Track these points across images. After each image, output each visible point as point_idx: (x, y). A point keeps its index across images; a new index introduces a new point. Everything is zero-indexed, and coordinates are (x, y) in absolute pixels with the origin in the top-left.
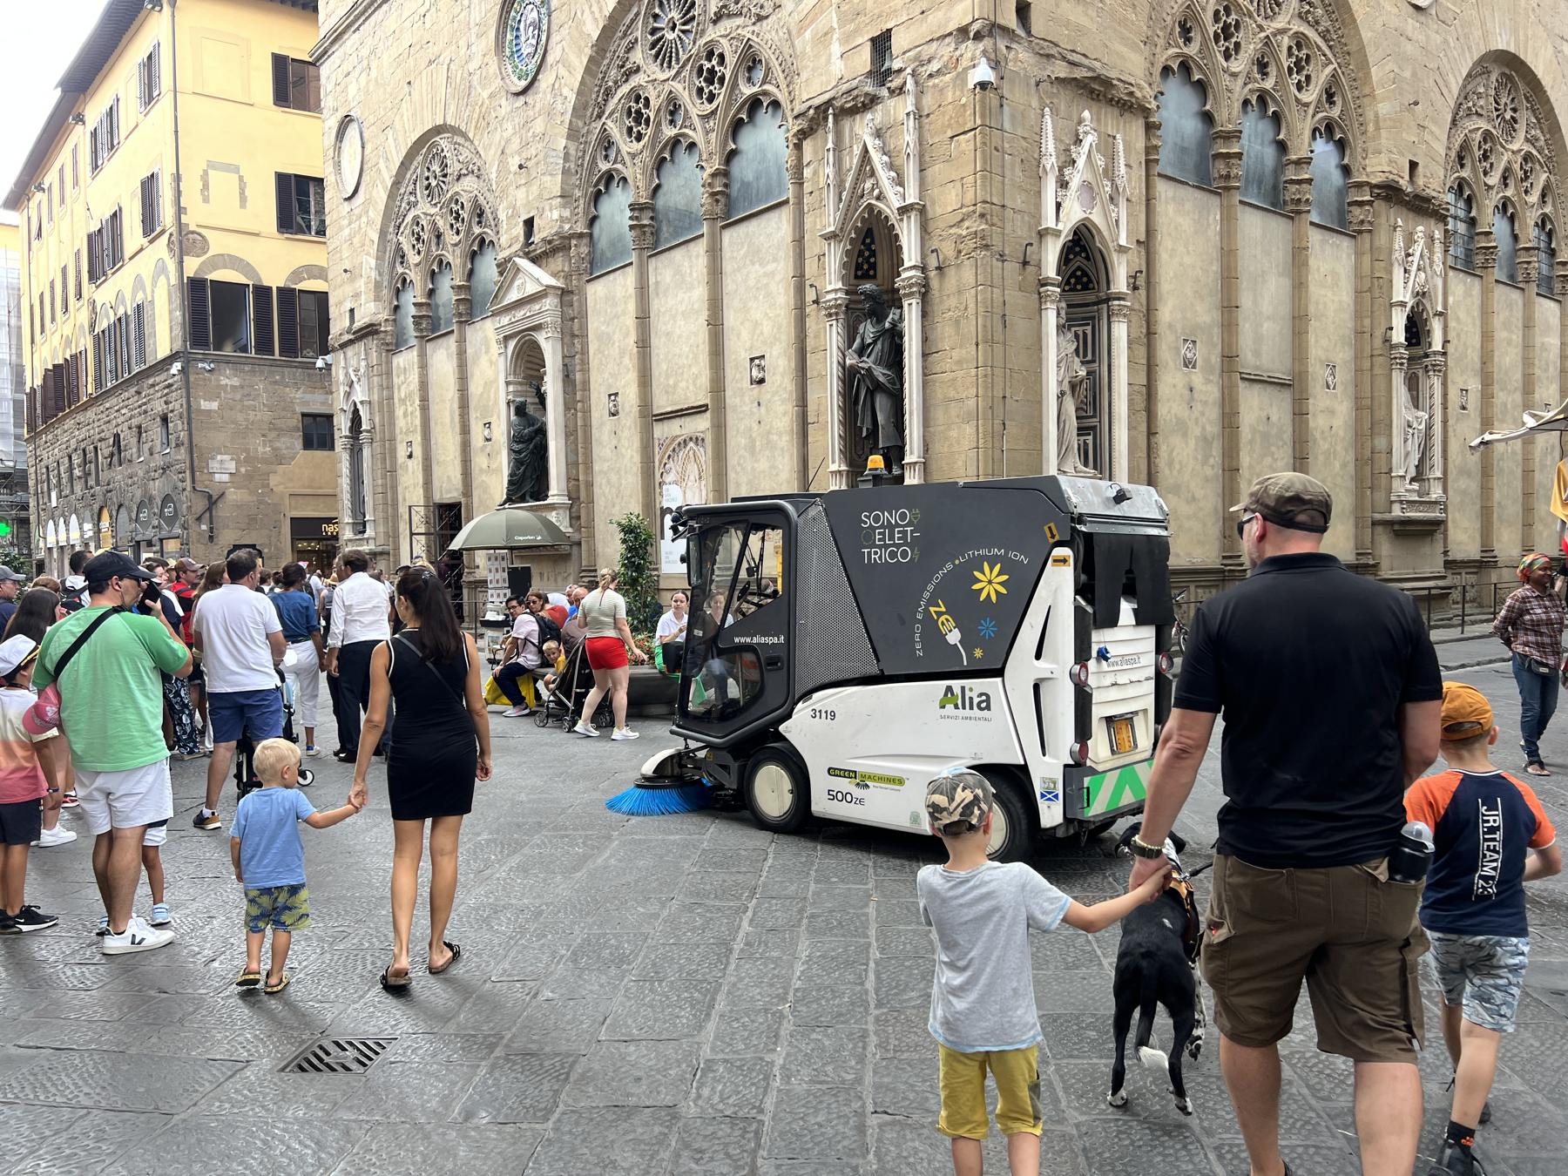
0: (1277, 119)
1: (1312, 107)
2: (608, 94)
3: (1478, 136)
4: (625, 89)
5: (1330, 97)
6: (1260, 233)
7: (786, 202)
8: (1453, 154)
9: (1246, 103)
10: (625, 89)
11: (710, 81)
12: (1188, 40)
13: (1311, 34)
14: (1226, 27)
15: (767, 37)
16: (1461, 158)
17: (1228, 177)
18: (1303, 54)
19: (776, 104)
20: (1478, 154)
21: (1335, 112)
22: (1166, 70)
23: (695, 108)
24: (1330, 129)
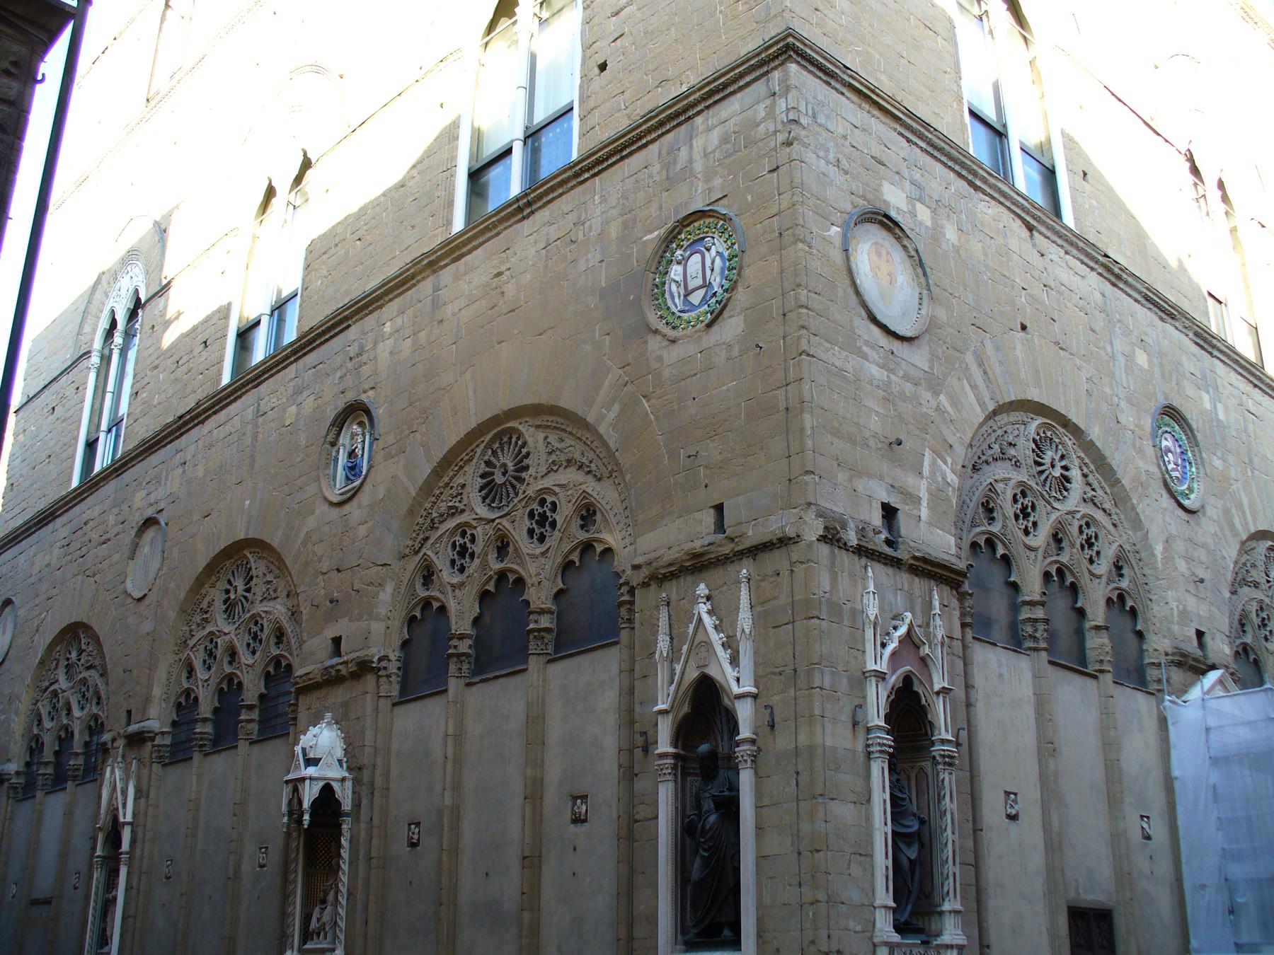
0: (1074, 589)
1: (1104, 579)
2: (433, 527)
3: (1253, 607)
4: (451, 524)
5: (1119, 568)
6: (1073, 694)
7: (616, 643)
8: (1236, 623)
9: (1047, 575)
10: (451, 524)
11: (541, 523)
12: (992, 519)
13: (1099, 515)
14: (1024, 509)
15: (604, 494)
16: (1243, 625)
17: (1035, 639)
18: (1091, 531)
19: (608, 551)
20: (1257, 621)
21: (1124, 584)
22: (974, 545)
23: (526, 546)
24: (1121, 598)
